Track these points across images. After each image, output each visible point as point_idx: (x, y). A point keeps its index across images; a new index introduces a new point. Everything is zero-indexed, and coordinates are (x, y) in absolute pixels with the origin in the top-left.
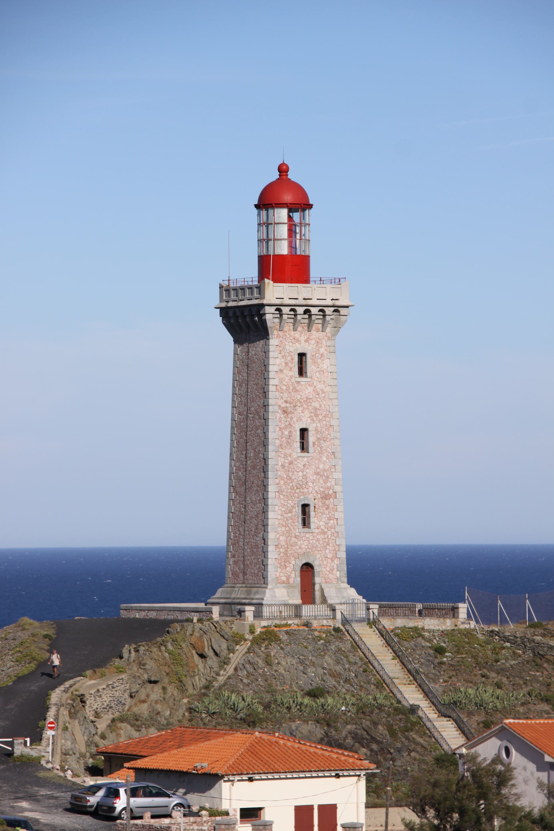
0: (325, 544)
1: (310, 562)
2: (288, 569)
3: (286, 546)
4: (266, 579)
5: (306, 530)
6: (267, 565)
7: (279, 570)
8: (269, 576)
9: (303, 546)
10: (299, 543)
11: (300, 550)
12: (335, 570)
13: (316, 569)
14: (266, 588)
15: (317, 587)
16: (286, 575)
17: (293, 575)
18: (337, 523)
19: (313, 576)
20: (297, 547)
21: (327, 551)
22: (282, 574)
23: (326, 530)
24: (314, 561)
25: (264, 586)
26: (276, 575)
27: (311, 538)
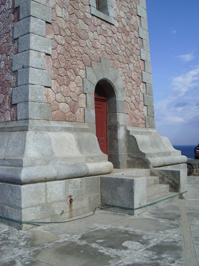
0: (128, 52)
1: (110, 78)
2: (73, 85)
3: (68, 33)
4: (20, 107)
5: (102, 15)
6: (26, 67)
7: (54, 84)
8: (30, 97)
9: (98, 45)
10: (91, 35)
11: (93, 52)
12: (142, 103)
13: (120, 97)
14: (25, 129)
15: (121, 134)
16: (69, 100)
17: (82, 103)
18: (141, 23)
19: (114, 111)
20: (90, 45)
21: (131, 66)
22: (59, 96)
23: (128, 28)
24: (115, 80)
25: (14, 124)
26: (47, 96)
27: (110, 33)
